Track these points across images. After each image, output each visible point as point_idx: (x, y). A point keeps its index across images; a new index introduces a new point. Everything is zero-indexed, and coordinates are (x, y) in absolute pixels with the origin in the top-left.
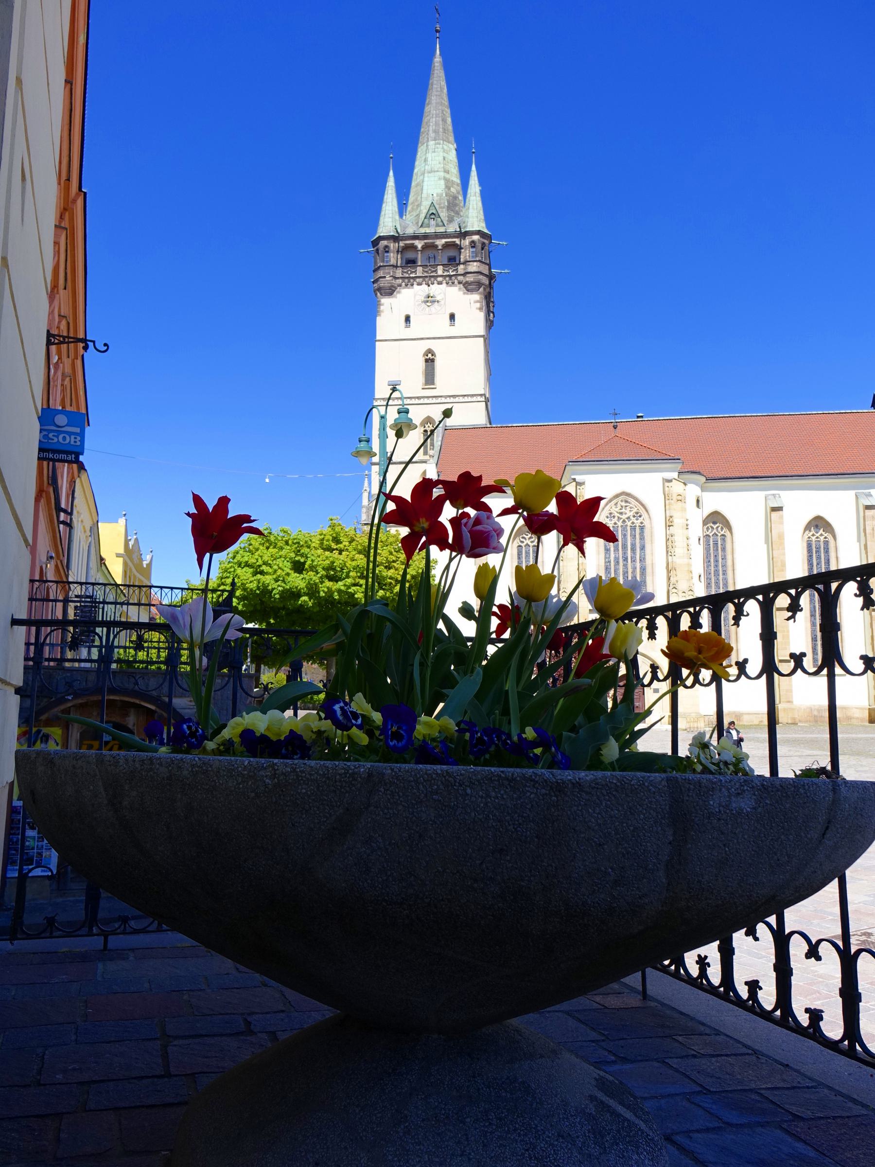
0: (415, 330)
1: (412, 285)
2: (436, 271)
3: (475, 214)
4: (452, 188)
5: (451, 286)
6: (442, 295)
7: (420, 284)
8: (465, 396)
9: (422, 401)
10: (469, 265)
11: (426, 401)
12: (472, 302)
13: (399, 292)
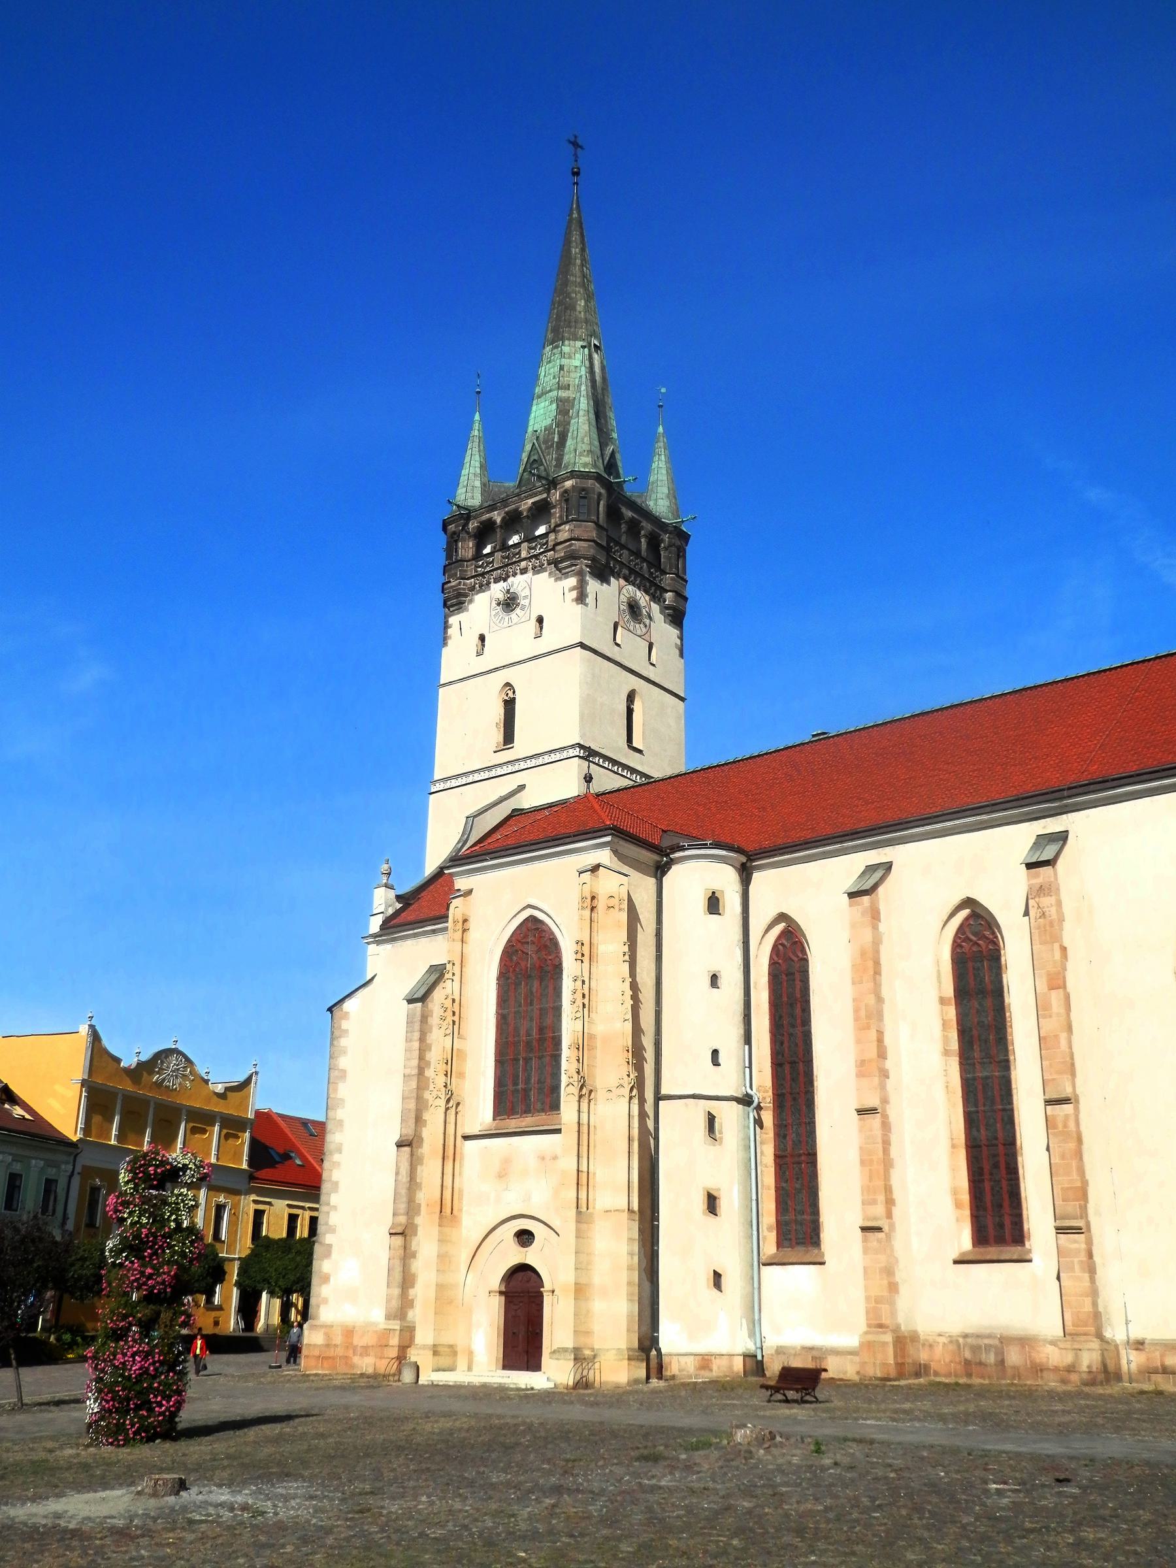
0: (491, 658)
1: (488, 583)
2: (519, 553)
3: (572, 448)
5: (538, 572)
6: (528, 588)
7: (496, 581)
8: (551, 752)
9: (493, 773)
10: (559, 531)
11: (499, 771)
12: (566, 591)
13: (471, 601)
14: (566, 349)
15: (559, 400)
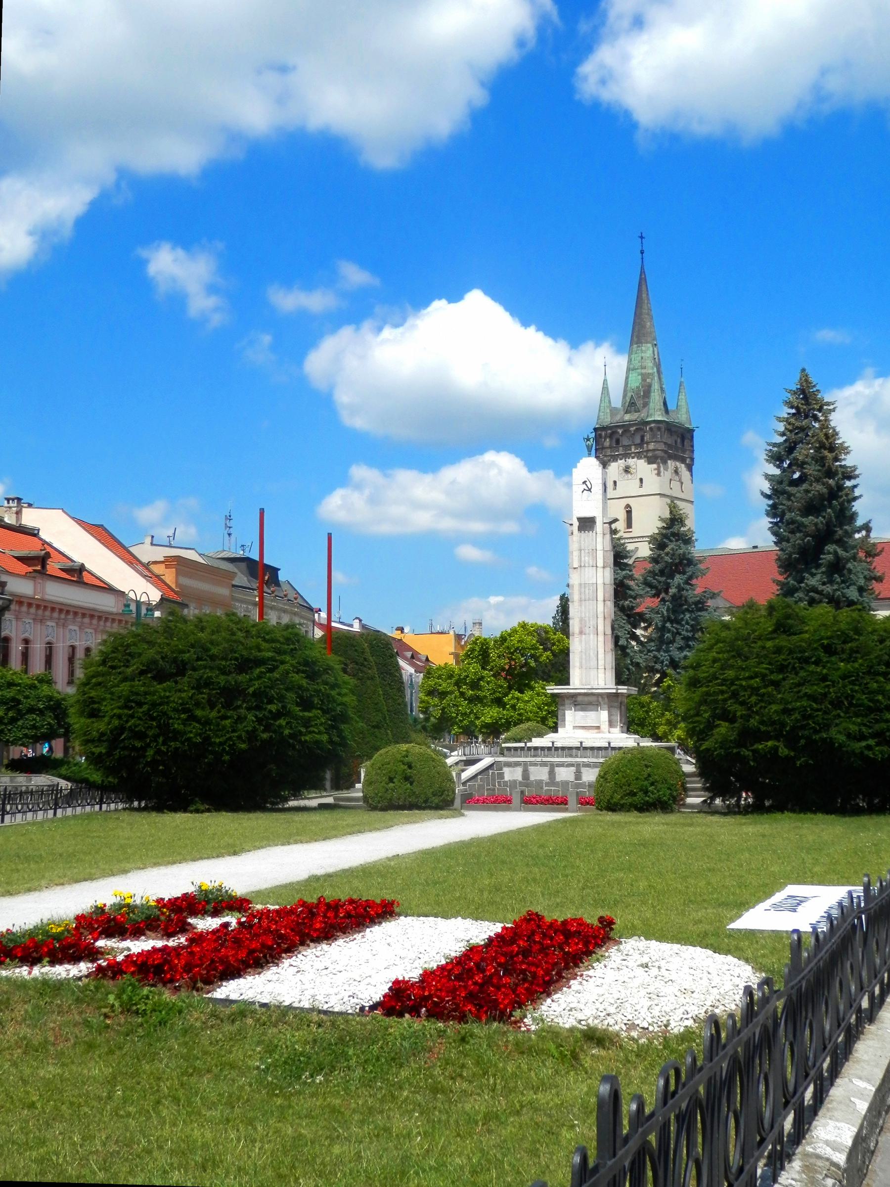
4: (648, 380)
14: (643, 348)
15: (642, 374)
